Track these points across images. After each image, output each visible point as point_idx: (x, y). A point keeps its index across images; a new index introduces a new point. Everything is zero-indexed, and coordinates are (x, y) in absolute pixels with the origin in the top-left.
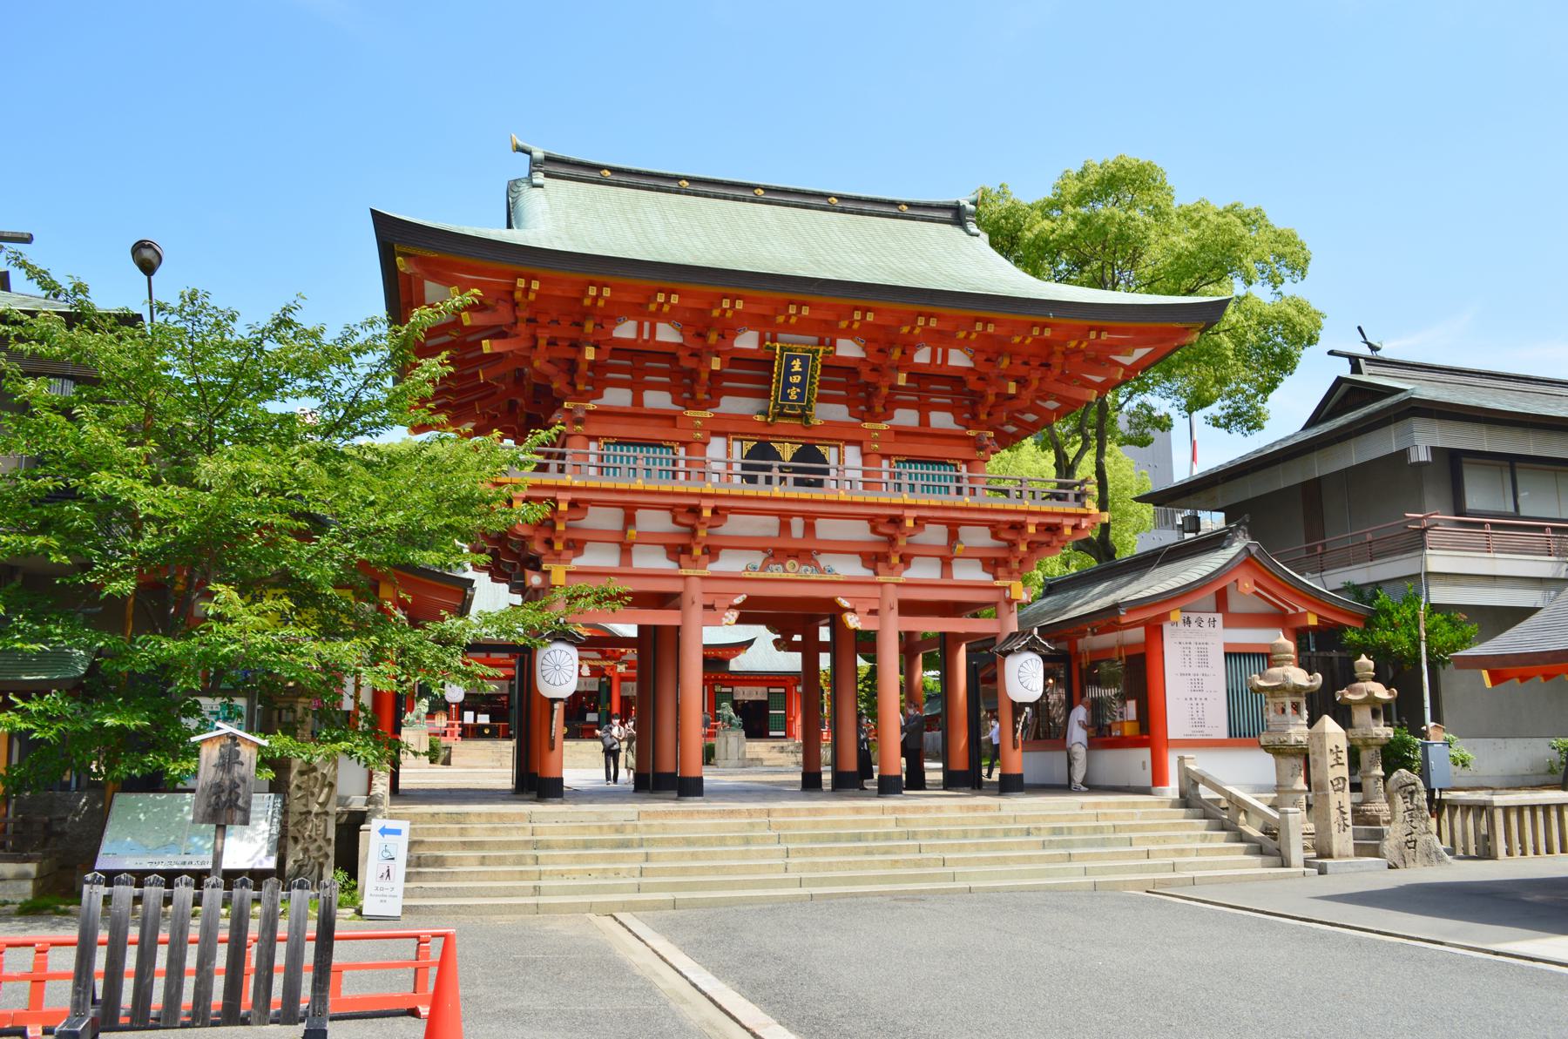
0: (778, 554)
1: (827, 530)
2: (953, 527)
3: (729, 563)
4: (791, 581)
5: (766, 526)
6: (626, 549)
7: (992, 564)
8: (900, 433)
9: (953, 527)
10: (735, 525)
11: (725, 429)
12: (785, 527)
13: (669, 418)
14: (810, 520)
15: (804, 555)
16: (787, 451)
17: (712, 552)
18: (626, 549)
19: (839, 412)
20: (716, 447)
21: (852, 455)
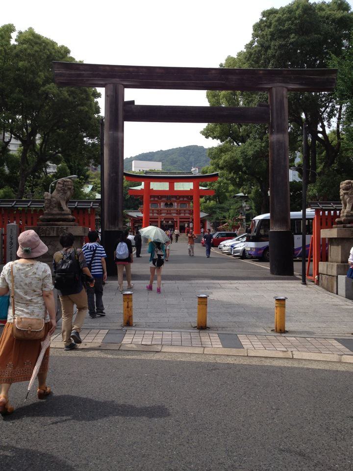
0: (167, 214)
1: (172, 212)
2: (185, 211)
3: (163, 215)
4: (168, 216)
5: (166, 211)
6: (153, 214)
7: (189, 214)
8: (181, 201)
9: (185, 211)
10: (162, 212)
11: (163, 201)
12: (168, 211)
13: (157, 201)
14: (170, 211)
15: (171, 214)
16: (169, 203)
17: (161, 214)
18: (153, 214)
19: (174, 199)
20: (162, 204)
21: (176, 204)
